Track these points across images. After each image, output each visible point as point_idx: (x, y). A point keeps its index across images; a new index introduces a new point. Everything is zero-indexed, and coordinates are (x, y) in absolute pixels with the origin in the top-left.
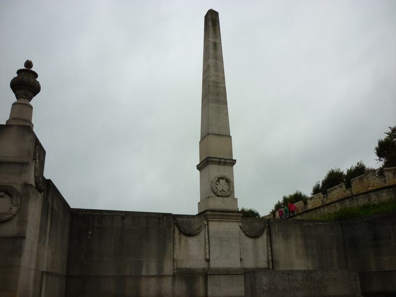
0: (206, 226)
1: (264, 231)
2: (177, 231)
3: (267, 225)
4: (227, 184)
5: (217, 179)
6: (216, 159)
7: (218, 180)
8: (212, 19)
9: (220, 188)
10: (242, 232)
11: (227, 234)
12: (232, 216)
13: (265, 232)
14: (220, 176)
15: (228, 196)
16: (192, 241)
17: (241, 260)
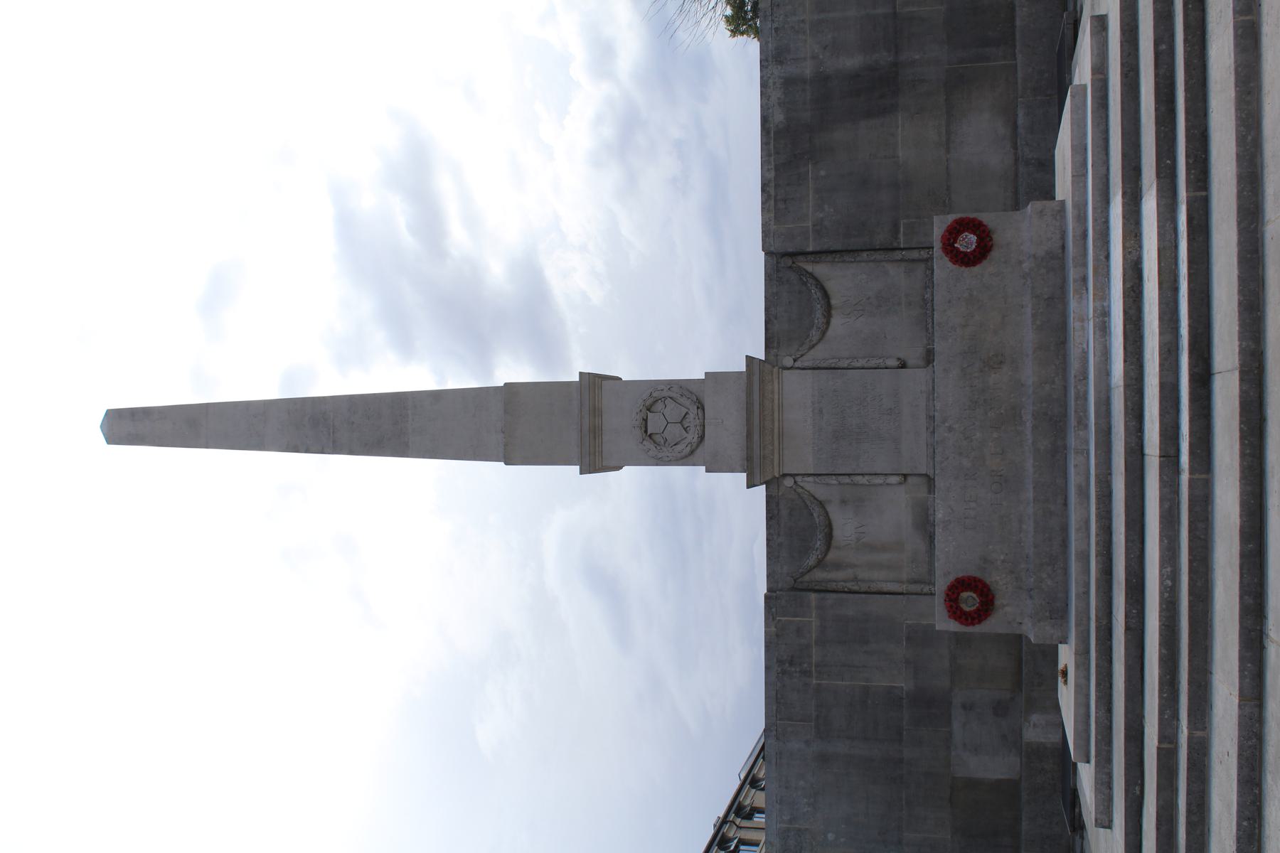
0: (799, 479)
1: (812, 275)
2: (819, 575)
3: (789, 261)
4: (660, 406)
5: (648, 444)
6: (579, 424)
7: (650, 436)
8: (129, 426)
9: (674, 431)
10: (812, 352)
11: (821, 411)
12: (762, 405)
13: (809, 268)
14: (638, 433)
15: (701, 407)
16: (845, 526)
17: (903, 365)
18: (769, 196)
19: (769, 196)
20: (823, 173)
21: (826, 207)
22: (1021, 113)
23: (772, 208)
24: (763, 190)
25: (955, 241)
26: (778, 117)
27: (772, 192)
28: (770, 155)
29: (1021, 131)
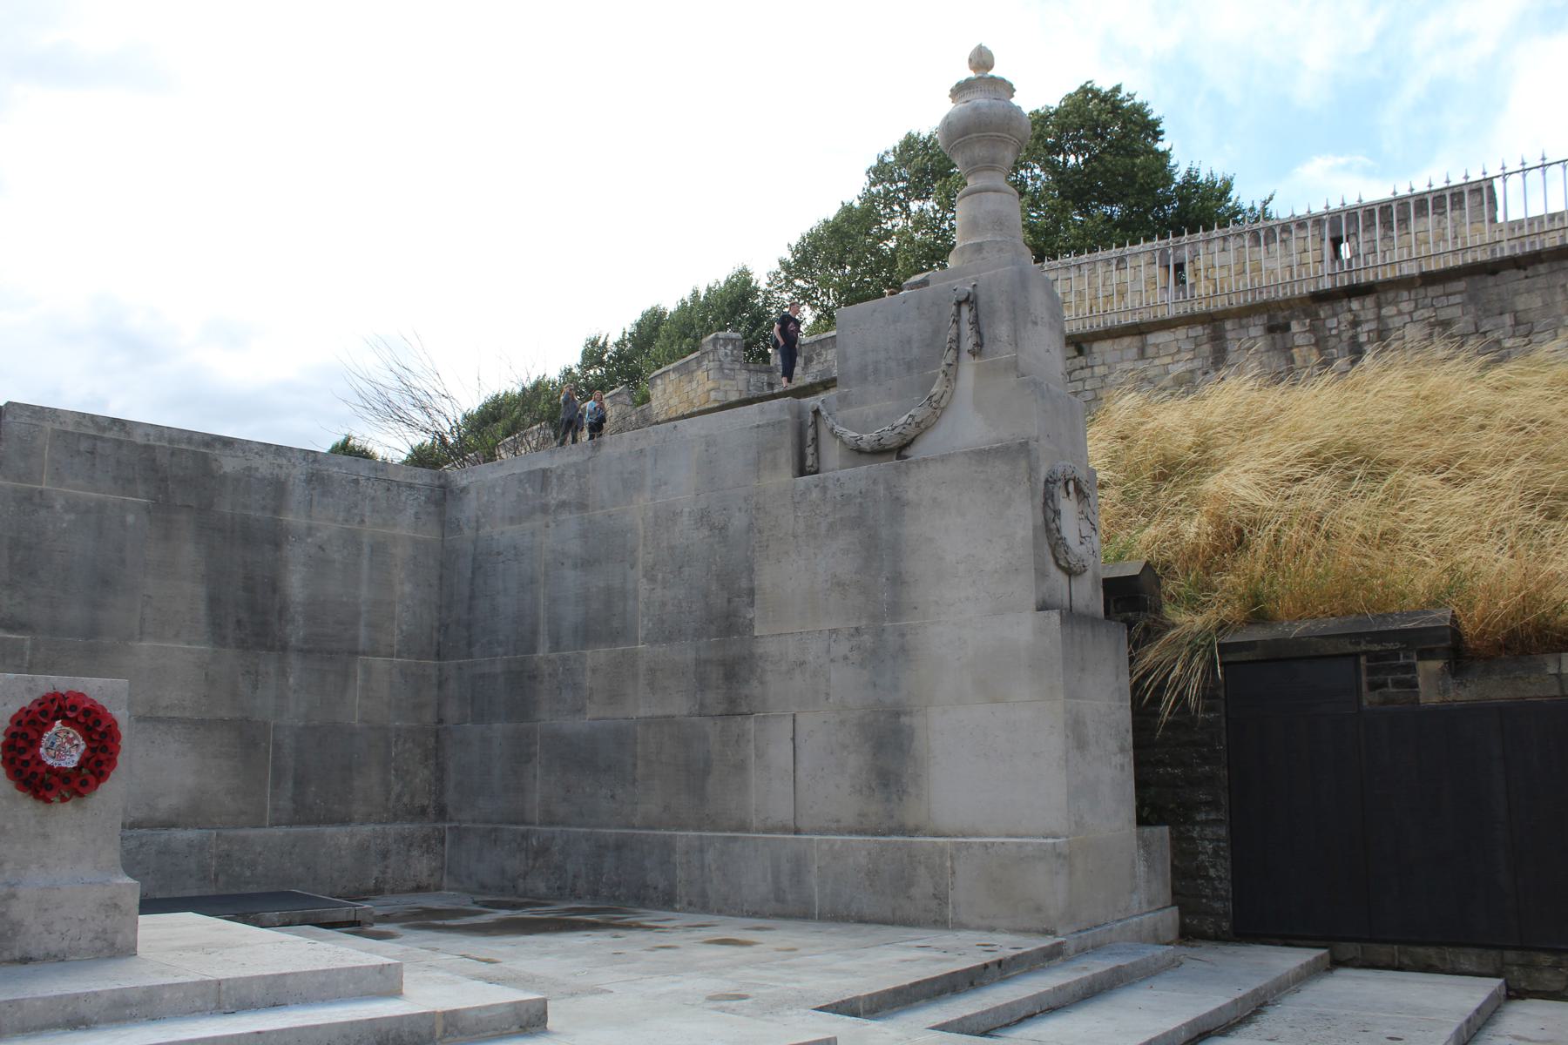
18: (104, 429)
19: (104, 429)
20: (130, 519)
21: (72, 516)
22: (192, 834)
23: (83, 430)
24: (115, 421)
25: (67, 722)
26: (229, 464)
27: (107, 435)
28: (171, 441)
29: (164, 835)
